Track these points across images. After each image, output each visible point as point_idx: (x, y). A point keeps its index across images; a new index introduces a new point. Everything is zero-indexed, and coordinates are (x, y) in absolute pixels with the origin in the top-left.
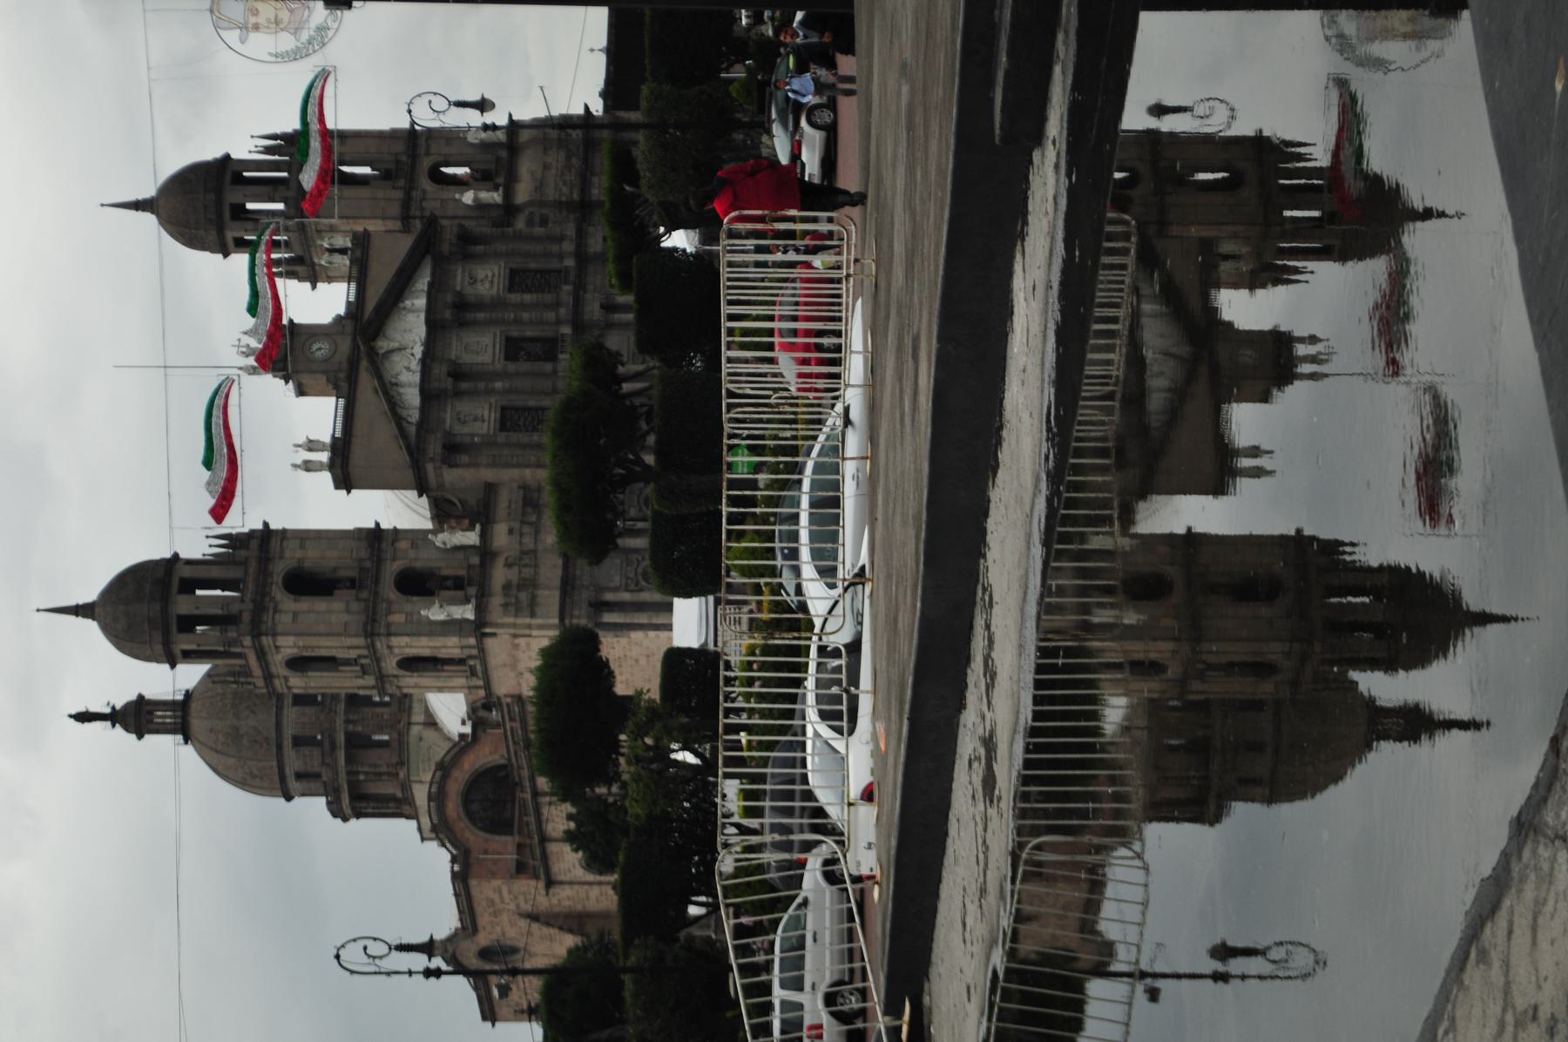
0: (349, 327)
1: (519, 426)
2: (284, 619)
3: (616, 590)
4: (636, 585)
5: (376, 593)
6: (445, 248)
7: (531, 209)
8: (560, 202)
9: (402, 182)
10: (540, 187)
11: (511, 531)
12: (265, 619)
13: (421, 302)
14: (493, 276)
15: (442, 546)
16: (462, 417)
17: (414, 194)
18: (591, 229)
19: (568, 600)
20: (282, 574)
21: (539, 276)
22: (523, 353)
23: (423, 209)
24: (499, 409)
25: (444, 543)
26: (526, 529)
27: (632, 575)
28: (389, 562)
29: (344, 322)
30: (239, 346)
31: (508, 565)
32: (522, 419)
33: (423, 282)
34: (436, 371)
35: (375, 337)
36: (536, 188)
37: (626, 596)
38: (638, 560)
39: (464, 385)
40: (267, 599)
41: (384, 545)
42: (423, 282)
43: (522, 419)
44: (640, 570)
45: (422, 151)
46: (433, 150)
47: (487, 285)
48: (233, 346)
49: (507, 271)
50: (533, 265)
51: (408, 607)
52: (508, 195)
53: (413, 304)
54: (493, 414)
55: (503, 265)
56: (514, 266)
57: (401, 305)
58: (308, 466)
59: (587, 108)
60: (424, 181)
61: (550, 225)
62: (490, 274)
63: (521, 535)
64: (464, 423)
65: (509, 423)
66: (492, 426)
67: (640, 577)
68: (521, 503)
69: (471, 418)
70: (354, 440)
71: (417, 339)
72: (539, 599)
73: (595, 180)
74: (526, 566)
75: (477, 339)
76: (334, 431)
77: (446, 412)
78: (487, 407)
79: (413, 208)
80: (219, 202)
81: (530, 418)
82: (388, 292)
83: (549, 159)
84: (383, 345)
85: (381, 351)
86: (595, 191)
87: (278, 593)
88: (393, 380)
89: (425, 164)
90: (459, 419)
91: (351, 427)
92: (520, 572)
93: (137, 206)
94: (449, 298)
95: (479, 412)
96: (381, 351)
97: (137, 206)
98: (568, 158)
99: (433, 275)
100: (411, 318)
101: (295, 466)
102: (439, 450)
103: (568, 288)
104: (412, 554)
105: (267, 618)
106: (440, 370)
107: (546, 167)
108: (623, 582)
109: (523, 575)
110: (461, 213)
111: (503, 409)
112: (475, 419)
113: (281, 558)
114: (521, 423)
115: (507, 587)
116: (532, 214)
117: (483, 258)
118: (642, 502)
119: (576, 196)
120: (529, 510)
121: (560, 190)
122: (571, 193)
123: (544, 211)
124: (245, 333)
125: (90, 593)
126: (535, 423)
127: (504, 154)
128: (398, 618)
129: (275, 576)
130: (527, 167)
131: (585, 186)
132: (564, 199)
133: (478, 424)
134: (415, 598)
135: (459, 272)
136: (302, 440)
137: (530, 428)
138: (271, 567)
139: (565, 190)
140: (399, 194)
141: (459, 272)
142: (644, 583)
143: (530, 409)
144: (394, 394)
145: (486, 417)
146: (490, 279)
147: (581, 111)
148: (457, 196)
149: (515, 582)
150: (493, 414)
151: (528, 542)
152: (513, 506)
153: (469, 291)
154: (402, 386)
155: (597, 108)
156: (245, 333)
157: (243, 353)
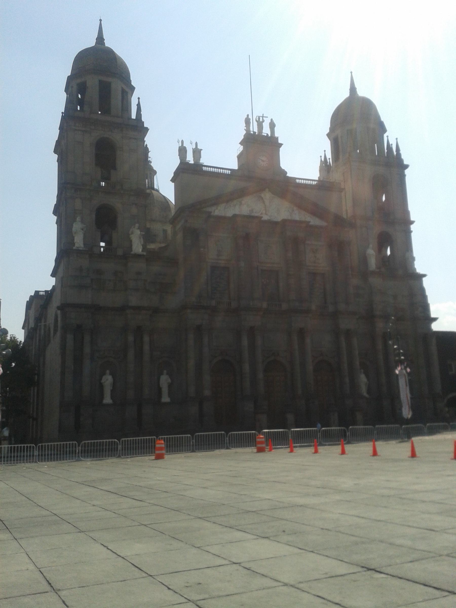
15: (130, 233)
25: (132, 233)
30: (263, 117)
37: (87, 350)
48: (263, 114)
57: (295, 208)
58: (182, 151)
59: (435, 319)
76: (207, 166)
84: (267, 195)
85: (263, 195)
88: (243, 202)
93: (353, 89)
96: (263, 195)
97: (353, 89)
101: (182, 142)
124: (272, 120)
134: (94, 216)
136: (199, 147)
148: (371, 246)
157: (259, 119)
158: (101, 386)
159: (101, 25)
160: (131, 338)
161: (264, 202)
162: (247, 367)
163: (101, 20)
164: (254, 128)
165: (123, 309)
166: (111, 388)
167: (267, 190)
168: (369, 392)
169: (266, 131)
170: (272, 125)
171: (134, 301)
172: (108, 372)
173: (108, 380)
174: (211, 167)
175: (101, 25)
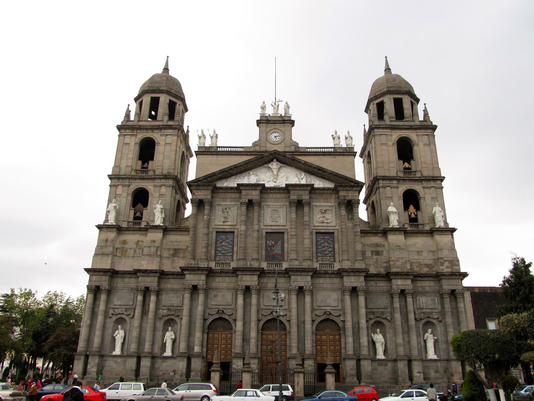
0: (293, 149)
1: (222, 243)
2: (127, 139)
3: (108, 302)
4: (112, 314)
5: (135, 179)
6: (342, 193)
7: (386, 245)
8: (389, 261)
9: (401, 175)
10: (399, 248)
11: (154, 241)
12: (127, 131)
13: (303, 182)
14: (328, 223)
16: (227, 210)
17: (395, 182)
18: (362, 279)
19: (101, 273)
20: (151, 137)
21: (330, 250)
22: (273, 243)
23: (385, 187)
24: (232, 230)
26: (153, 250)
27: (119, 311)
28: (152, 184)
29: (293, 147)
31: (137, 243)
32: (226, 244)
33: (318, 183)
34: (254, 192)
35: (278, 160)
36: (399, 246)
37: (102, 307)
38: (130, 314)
39: (244, 208)
40: (139, 131)
41: (163, 181)
42: (318, 183)
43: (226, 244)
44: (124, 316)
45: (425, 184)
46: (426, 190)
47: (320, 220)
49: (331, 231)
50: (336, 245)
51: (125, 195)
52: (394, 230)
53: (302, 179)
54: (229, 227)
55: (336, 228)
56: (336, 234)
58: (202, 137)
59: (465, 275)
60: (404, 187)
61: (375, 257)
62: (328, 221)
63: (149, 247)
64: (223, 212)
65: (224, 237)
66: (220, 227)
67: (119, 316)
68: (177, 247)
69: (226, 216)
70: (215, 157)
71: (280, 184)
72: (106, 258)
73: (409, 282)
74: (135, 251)
75: (281, 216)
77: (230, 202)
78: (234, 223)
79: (384, 182)
80: (383, 94)
81: (226, 248)
82: (305, 163)
83: (425, 254)
86: (399, 282)
87: (141, 135)
89: (417, 187)
90: (226, 209)
91: (223, 155)
92: (131, 249)
94: (305, 197)
95: (230, 219)
96: (270, 165)
98: (427, 266)
99: (324, 189)
100: (297, 179)
102: (199, 197)
103: (316, 265)
104: (157, 194)
105: (128, 132)
106: (255, 195)
107: (419, 252)
108: (117, 307)
109: (129, 250)
110: (383, 208)
111: (234, 232)
112: (225, 217)
113: (161, 135)
114: (224, 243)
115: (124, 242)
116: (384, 246)
117: (339, 217)
118: (169, 317)
119: (394, 270)
120: (172, 252)
121: (398, 261)
122: (397, 267)
123: (385, 253)
124: (286, 103)
125: (172, 73)
126: (223, 252)
127: (427, 228)
128: (120, 190)
129: (152, 134)
130: (419, 242)
131: (398, 275)
132: (391, 263)
133: (223, 220)
134: (130, 198)
135: (330, 204)
137: (219, 249)
138: (157, 131)
139: (398, 263)
140: (393, 174)
141: (330, 204)
142: (114, 318)
143: (233, 248)
144: (245, 173)
145: (226, 224)
146: (325, 221)
147: (463, 270)
149: (126, 246)
150: (229, 227)
151: (146, 250)
152: (176, 244)
153: (316, 211)
154: (249, 179)
155: (466, 283)
156: (286, 103)
158: (114, 339)
159: (167, 60)
160: (140, 298)
161: (272, 172)
162: (239, 326)
163: (168, 57)
164: (270, 111)
165: (135, 273)
166: (122, 341)
167: (275, 160)
168: (385, 352)
169: (282, 112)
170: (287, 107)
171: (145, 265)
172: (119, 326)
173: (119, 335)
174: (225, 147)
175: (167, 60)
